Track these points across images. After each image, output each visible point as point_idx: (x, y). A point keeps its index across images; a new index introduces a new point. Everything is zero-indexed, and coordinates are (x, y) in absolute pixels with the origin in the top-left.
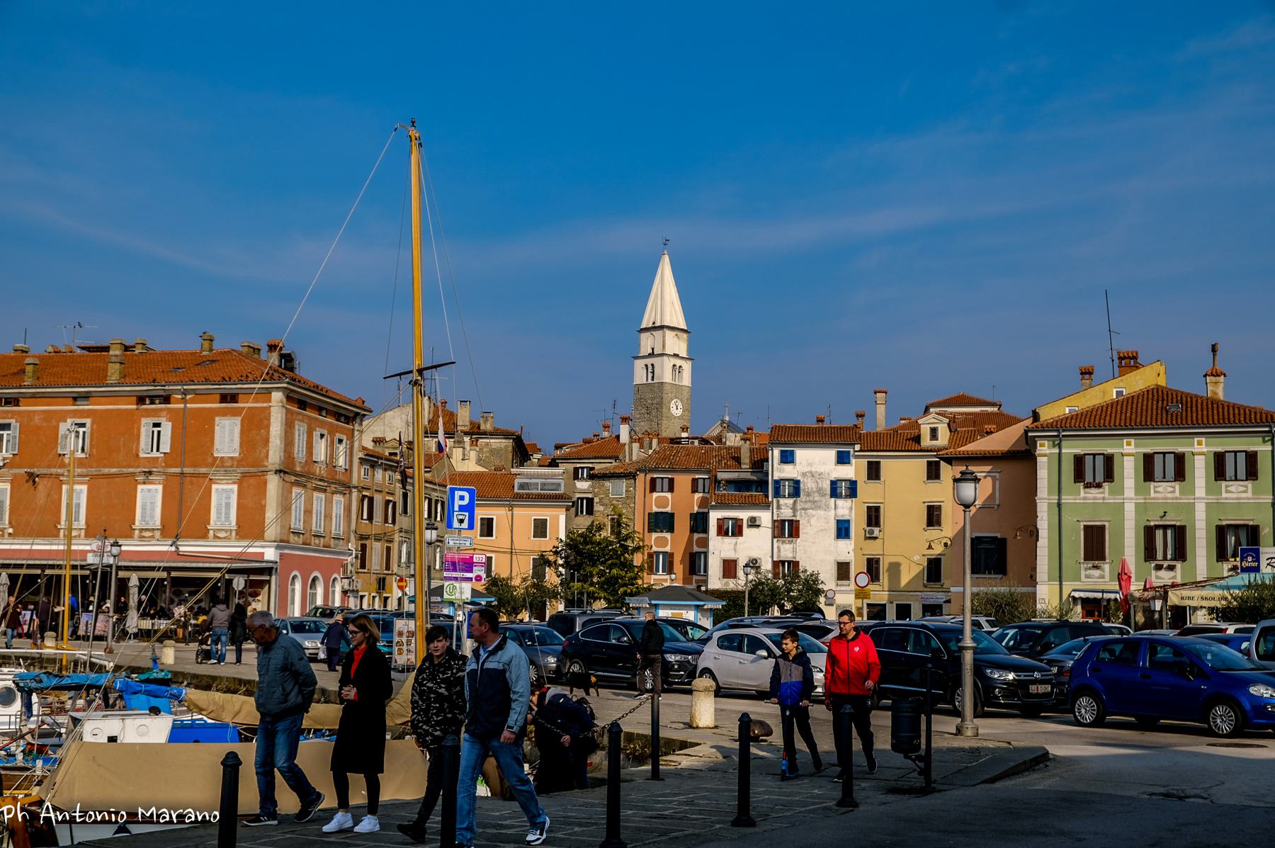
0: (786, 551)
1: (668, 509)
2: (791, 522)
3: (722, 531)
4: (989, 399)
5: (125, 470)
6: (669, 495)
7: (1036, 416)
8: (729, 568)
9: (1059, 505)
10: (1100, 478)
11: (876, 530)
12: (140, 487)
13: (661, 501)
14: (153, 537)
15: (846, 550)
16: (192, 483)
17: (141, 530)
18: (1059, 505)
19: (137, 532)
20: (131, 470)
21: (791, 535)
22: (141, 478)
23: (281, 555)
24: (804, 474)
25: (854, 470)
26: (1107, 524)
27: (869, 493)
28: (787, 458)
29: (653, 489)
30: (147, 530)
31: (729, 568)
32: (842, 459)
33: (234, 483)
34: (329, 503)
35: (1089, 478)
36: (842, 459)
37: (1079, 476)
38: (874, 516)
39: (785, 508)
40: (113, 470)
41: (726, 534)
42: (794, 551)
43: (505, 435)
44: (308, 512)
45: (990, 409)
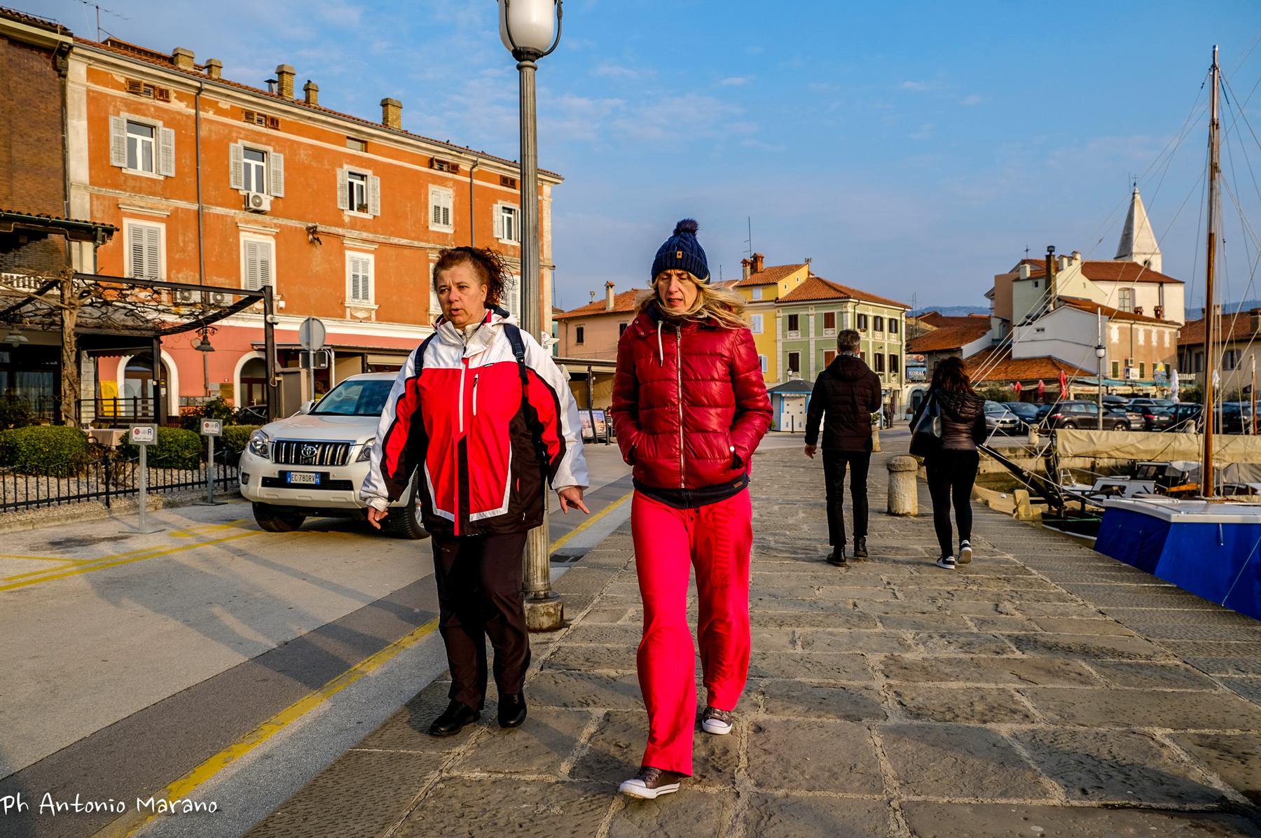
5: (416, 244)
20: (423, 244)
40: (404, 242)
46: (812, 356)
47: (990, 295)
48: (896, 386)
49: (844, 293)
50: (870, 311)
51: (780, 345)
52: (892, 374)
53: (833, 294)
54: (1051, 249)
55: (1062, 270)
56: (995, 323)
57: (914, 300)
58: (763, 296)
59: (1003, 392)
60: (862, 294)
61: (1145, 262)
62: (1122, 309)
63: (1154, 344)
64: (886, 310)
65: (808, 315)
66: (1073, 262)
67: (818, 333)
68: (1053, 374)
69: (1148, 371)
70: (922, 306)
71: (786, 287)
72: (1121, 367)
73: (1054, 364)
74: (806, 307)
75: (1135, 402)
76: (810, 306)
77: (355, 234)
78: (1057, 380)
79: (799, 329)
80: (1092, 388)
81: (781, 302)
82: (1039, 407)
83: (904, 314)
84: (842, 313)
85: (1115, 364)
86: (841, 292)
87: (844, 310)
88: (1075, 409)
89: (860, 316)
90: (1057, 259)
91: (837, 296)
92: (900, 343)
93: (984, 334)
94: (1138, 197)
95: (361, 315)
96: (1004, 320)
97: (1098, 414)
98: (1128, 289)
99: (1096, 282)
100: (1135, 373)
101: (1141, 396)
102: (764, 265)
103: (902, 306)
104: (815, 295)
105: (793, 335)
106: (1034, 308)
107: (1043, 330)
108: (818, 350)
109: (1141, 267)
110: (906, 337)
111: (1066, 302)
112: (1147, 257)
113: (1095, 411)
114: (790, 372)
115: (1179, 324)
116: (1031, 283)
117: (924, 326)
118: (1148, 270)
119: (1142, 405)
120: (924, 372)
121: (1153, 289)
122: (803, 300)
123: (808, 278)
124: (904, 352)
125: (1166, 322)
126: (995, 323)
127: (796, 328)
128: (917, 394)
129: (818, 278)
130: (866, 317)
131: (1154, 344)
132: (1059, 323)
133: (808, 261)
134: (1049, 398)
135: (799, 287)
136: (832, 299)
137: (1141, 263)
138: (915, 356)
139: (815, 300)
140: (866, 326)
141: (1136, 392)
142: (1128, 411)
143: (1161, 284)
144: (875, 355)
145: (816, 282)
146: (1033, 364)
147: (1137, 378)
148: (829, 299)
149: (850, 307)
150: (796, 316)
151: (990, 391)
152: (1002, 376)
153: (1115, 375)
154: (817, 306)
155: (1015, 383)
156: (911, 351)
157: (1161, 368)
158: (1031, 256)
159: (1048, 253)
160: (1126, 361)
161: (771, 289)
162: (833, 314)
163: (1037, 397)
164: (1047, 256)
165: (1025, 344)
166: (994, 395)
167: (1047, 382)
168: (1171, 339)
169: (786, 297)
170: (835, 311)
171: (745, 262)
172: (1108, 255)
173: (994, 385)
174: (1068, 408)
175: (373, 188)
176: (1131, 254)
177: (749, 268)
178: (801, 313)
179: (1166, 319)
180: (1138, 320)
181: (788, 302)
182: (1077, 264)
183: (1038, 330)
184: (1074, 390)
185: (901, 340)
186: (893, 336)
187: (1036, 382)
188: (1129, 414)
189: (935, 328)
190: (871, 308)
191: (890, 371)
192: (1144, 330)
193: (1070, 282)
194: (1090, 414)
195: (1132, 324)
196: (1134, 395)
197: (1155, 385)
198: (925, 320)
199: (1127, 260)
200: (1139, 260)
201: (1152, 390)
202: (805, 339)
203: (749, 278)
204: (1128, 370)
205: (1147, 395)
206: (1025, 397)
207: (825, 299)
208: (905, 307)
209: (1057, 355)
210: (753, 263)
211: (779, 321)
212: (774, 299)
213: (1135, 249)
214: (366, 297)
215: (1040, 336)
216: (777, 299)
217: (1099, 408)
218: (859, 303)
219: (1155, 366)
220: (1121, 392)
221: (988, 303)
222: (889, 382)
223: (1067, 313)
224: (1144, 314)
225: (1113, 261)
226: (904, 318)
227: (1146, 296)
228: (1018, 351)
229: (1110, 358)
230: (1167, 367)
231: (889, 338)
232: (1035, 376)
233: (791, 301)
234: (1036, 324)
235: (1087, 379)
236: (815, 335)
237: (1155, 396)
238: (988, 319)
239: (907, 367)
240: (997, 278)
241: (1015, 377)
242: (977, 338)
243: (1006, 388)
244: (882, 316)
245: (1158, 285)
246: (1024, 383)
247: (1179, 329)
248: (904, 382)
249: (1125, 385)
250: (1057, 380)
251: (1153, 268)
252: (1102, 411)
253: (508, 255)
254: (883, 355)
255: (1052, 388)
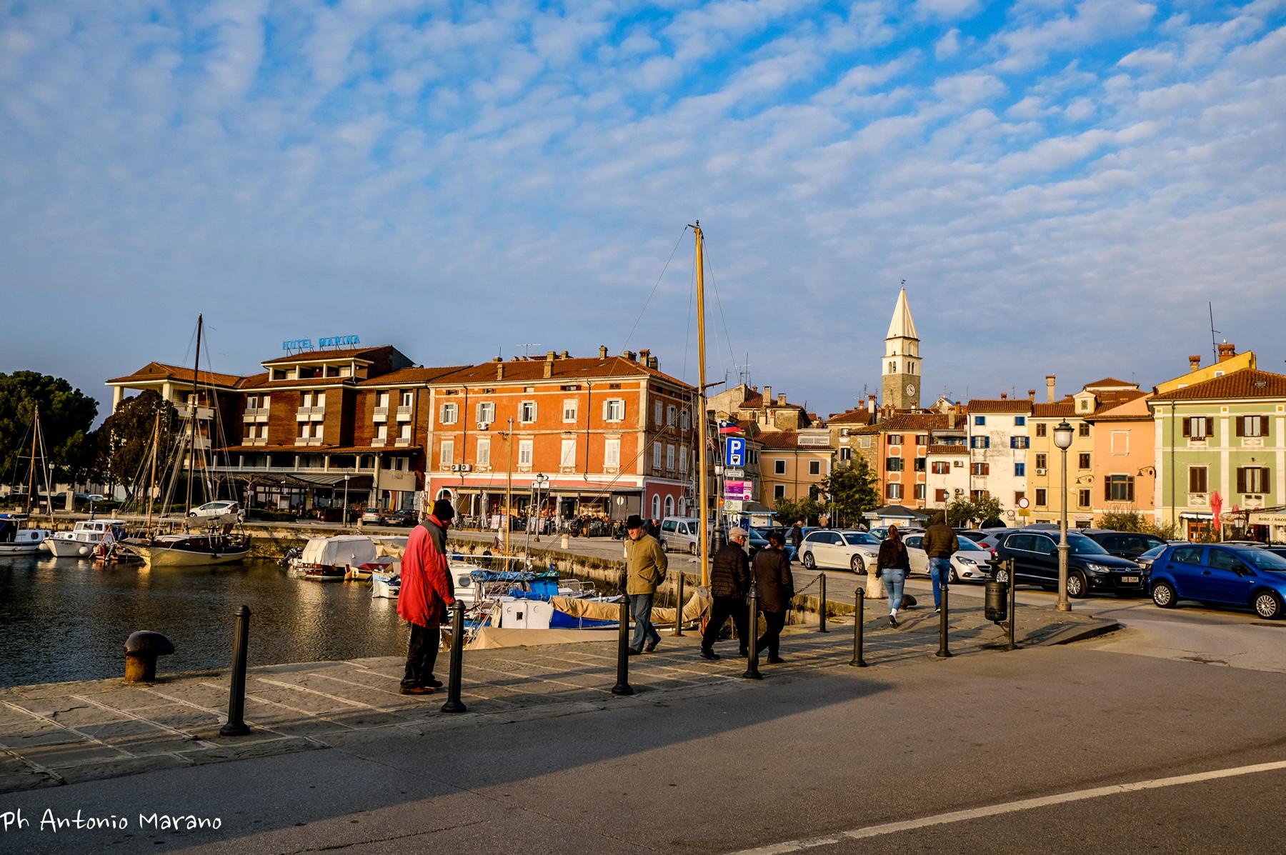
0: (979, 484)
1: (900, 456)
2: (983, 465)
3: (935, 470)
4: (1131, 382)
6: (900, 447)
7: (1155, 391)
8: (940, 495)
9: (1173, 452)
10: (1203, 434)
11: (1043, 471)
12: (563, 442)
13: (895, 451)
14: (571, 472)
15: (1021, 484)
16: (593, 439)
17: (564, 468)
18: (1173, 452)
19: (562, 469)
21: (982, 474)
22: (563, 436)
23: (649, 485)
24: (992, 433)
25: (1029, 429)
26: (1208, 467)
27: (1038, 445)
28: (981, 421)
29: (890, 442)
30: (567, 468)
31: (940, 495)
32: (1020, 422)
33: (618, 439)
34: (677, 451)
35: (1194, 434)
36: (1020, 422)
37: (1187, 431)
38: (1041, 461)
39: (979, 455)
40: (548, 432)
41: (938, 472)
42: (985, 484)
43: (794, 407)
44: (664, 457)
45: (1130, 388)
77: (524, 432)
95: (525, 470)
175: (533, 408)
214: (527, 461)
253: (612, 429)
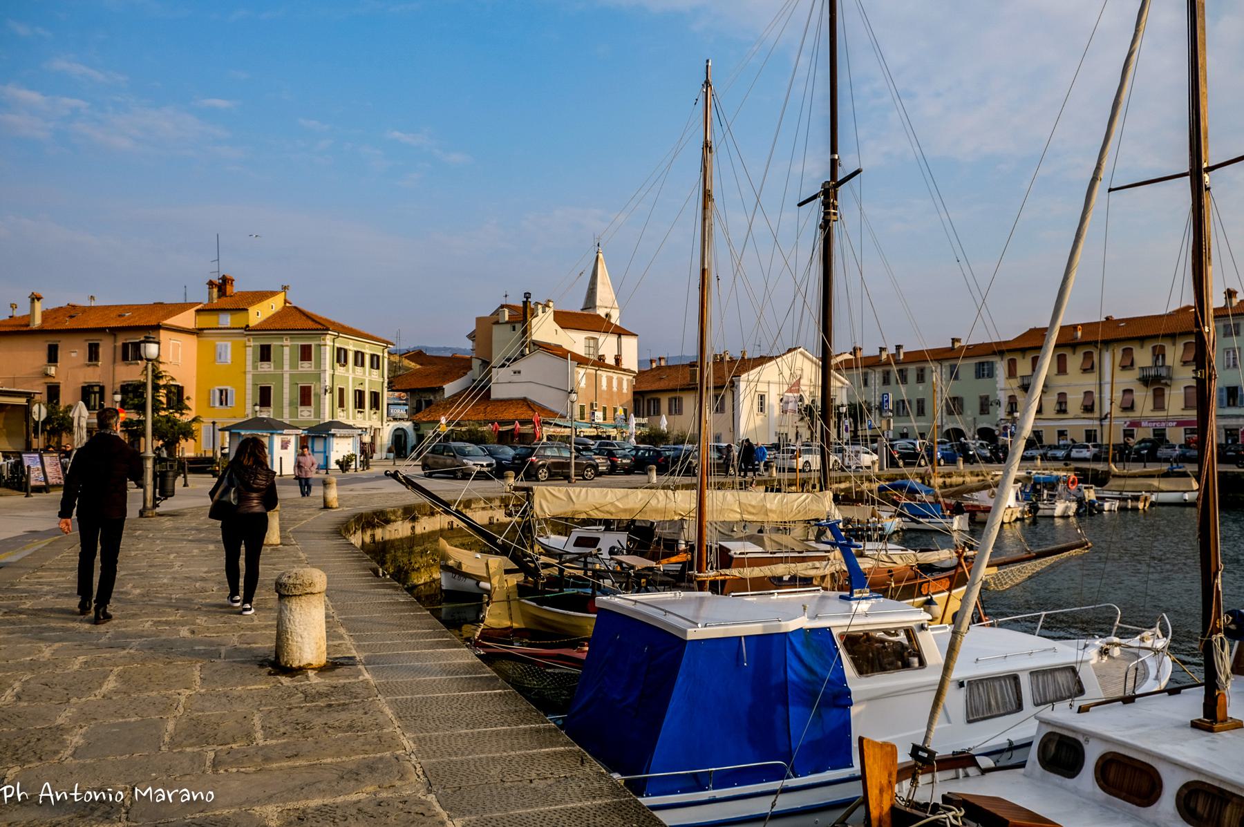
46: (286, 390)
47: (472, 336)
48: (377, 424)
49: (324, 326)
50: (351, 346)
51: (249, 377)
52: (372, 412)
53: (311, 324)
54: (527, 295)
55: (537, 316)
56: (476, 364)
57: (398, 337)
58: (231, 323)
59: (482, 432)
60: (343, 327)
61: (607, 315)
62: (587, 356)
63: (615, 389)
64: (367, 345)
65: (282, 346)
66: (547, 309)
67: (293, 365)
68: (527, 414)
69: (610, 414)
70: (409, 343)
71: (258, 314)
72: (587, 410)
73: (529, 406)
74: (280, 337)
75: (600, 445)
76: (285, 337)
78: (530, 422)
79: (272, 360)
80: (563, 430)
81: (252, 330)
82: (515, 448)
83: (386, 350)
84: (320, 345)
85: (582, 407)
86: (319, 324)
87: (322, 343)
88: (548, 453)
89: (339, 349)
90: (532, 306)
91: (311, 327)
92: (381, 380)
93: (465, 374)
94: (601, 256)
96: (484, 362)
97: (571, 458)
98: (593, 338)
99: (566, 330)
100: (599, 415)
101: (604, 438)
102: (237, 288)
103: (384, 342)
104: (291, 324)
105: (266, 367)
106: (513, 352)
107: (519, 372)
108: (293, 384)
109: (605, 320)
110: (389, 373)
111: (540, 347)
112: (608, 310)
113: (568, 455)
114: (257, 408)
115: (634, 372)
116: (509, 327)
117: (406, 362)
118: (609, 322)
119: (605, 446)
120: (406, 410)
121: (612, 339)
122: (276, 330)
123: (285, 306)
124: (386, 390)
125: (624, 370)
126: (476, 364)
127: (268, 359)
128: (397, 433)
129: (295, 307)
130: (346, 351)
131: (615, 389)
132: (534, 365)
133: (285, 288)
134: (523, 438)
135: (273, 315)
136: (309, 330)
137: (603, 315)
138: (397, 394)
139: (290, 330)
140: (346, 361)
141: (600, 434)
142: (596, 454)
143: (620, 335)
144: (356, 391)
145: (291, 311)
146: (510, 405)
147: (601, 421)
148: (306, 330)
149: (328, 340)
150: (268, 347)
151: (469, 431)
152: (481, 417)
153: (582, 417)
154: (292, 337)
155: (493, 424)
156: (394, 388)
157: (620, 412)
158: (510, 302)
159: (525, 299)
160: (592, 405)
161: (240, 316)
162: (310, 346)
163: (513, 437)
164: (524, 302)
165: (504, 385)
166: (474, 435)
167: (523, 423)
168: (628, 385)
169: (258, 325)
170: (313, 343)
171: (211, 284)
172: (576, 306)
173: (473, 425)
174: (542, 451)
176: (595, 307)
177: (215, 290)
178: (275, 343)
179: (623, 367)
180: (602, 367)
181: (260, 330)
182: (550, 312)
183: (515, 373)
184: (547, 431)
185: (383, 377)
186: (375, 372)
187: (512, 422)
188: (596, 457)
189: (418, 367)
190: (351, 342)
191: (371, 409)
192: (607, 377)
193: (544, 328)
194: (562, 457)
195: (596, 370)
196: (597, 437)
197: (615, 427)
198: (409, 358)
199: (591, 312)
200: (601, 312)
201: (613, 433)
202: (278, 372)
203: (215, 301)
204: (593, 414)
205: (609, 437)
206: (503, 438)
207: (301, 330)
208: (388, 343)
209: (531, 397)
210: (222, 286)
211: (250, 351)
212: (244, 326)
213: (598, 303)
215: (516, 378)
216: (248, 326)
217: (571, 453)
218: (338, 337)
219: (615, 410)
220: (587, 434)
221: (469, 345)
222: (370, 419)
223: (540, 358)
224: (606, 362)
225: (580, 312)
226: (386, 355)
227: (607, 346)
228: (497, 392)
229: (579, 400)
230: (625, 411)
231: (370, 374)
232: (512, 417)
233: (263, 330)
234: (515, 367)
235: (557, 421)
236: (290, 368)
237: (615, 438)
238: (469, 360)
239: (388, 404)
240: (479, 320)
241: (493, 417)
242: (458, 378)
243: (485, 428)
244: (363, 351)
245: (617, 336)
246: (502, 423)
247: (634, 377)
248: (385, 420)
249: (591, 427)
250: (530, 422)
251: (613, 321)
252: (573, 455)
254: (364, 392)
255: (527, 429)
